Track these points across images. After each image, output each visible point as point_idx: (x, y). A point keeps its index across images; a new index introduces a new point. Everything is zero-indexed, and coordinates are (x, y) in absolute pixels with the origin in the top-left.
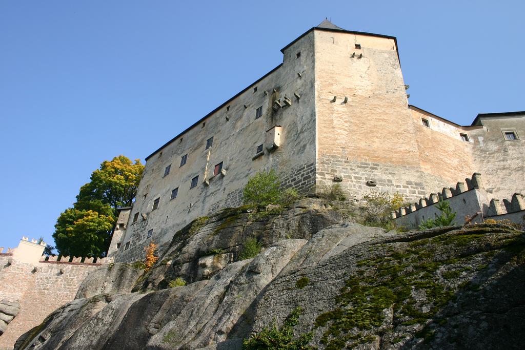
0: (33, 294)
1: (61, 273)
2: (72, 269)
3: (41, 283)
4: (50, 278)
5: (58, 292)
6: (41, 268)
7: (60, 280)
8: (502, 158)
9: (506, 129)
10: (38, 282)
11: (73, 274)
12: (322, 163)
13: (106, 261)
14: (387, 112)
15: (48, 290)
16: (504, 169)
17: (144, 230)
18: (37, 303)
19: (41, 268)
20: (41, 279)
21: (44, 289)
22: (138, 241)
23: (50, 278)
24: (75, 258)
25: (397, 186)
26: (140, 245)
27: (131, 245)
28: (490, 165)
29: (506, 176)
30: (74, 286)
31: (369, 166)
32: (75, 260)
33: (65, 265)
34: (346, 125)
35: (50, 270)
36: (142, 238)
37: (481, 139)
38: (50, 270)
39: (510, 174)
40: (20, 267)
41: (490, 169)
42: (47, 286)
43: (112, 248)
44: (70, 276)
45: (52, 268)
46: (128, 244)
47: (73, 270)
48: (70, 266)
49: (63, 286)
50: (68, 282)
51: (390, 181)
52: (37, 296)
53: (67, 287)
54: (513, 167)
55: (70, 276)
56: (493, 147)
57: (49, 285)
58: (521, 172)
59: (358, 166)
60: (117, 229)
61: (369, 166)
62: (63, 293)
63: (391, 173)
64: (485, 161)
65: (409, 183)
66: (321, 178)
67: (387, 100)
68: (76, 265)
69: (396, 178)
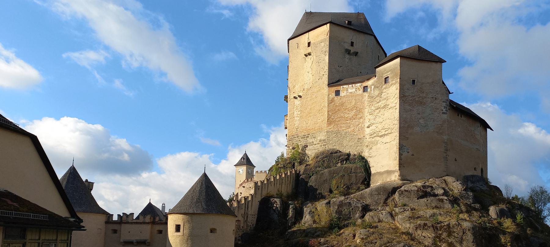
8: (378, 101)
9: (385, 75)
12: (289, 141)
14: (317, 96)
16: (377, 109)
25: (315, 144)
28: (373, 108)
29: (377, 114)
31: (306, 136)
34: (299, 113)
37: (373, 87)
39: (380, 111)
41: (372, 111)
51: (313, 142)
54: (383, 105)
56: (377, 92)
58: (384, 109)
59: (302, 138)
61: (306, 136)
63: (314, 138)
64: (371, 105)
65: (320, 141)
66: (288, 149)
67: (318, 87)
69: (315, 139)
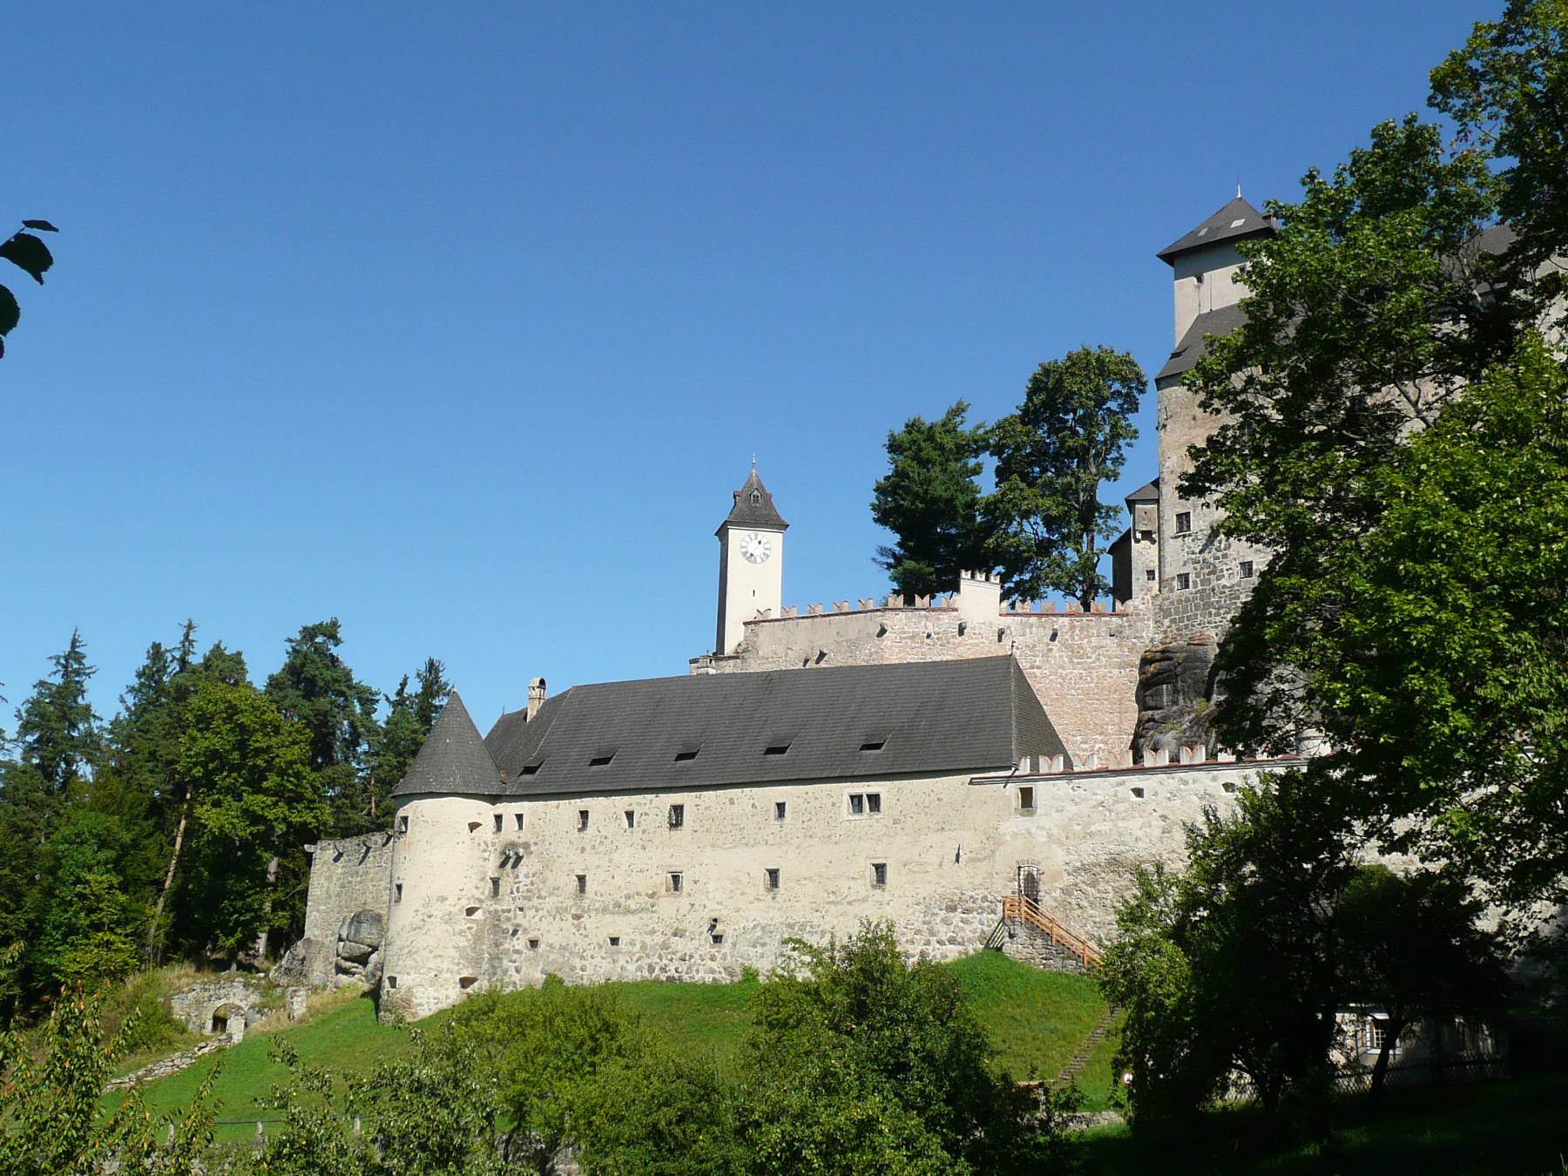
1: (1054, 637)
2: (1072, 628)
4: (1034, 646)
5: (1060, 671)
6: (1009, 627)
13: (1136, 608)
15: (1039, 668)
17: (1225, 556)
19: (1009, 627)
21: (1032, 667)
22: (1213, 577)
23: (1034, 646)
26: (1224, 587)
27: (1195, 583)
30: (1090, 658)
35: (1028, 630)
36: (1225, 573)
38: (1028, 630)
40: (977, 632)
42: (1035, 661)
43: (1138, 579)
44: (1073, 638)
45: (1031, 627)
46: (1184, 579)
49: (1066, 660)
50: (1073, 652)
53: (1075, 660)
55: (1073, 638)
60: (1137, 541)
62: (1071, 673)
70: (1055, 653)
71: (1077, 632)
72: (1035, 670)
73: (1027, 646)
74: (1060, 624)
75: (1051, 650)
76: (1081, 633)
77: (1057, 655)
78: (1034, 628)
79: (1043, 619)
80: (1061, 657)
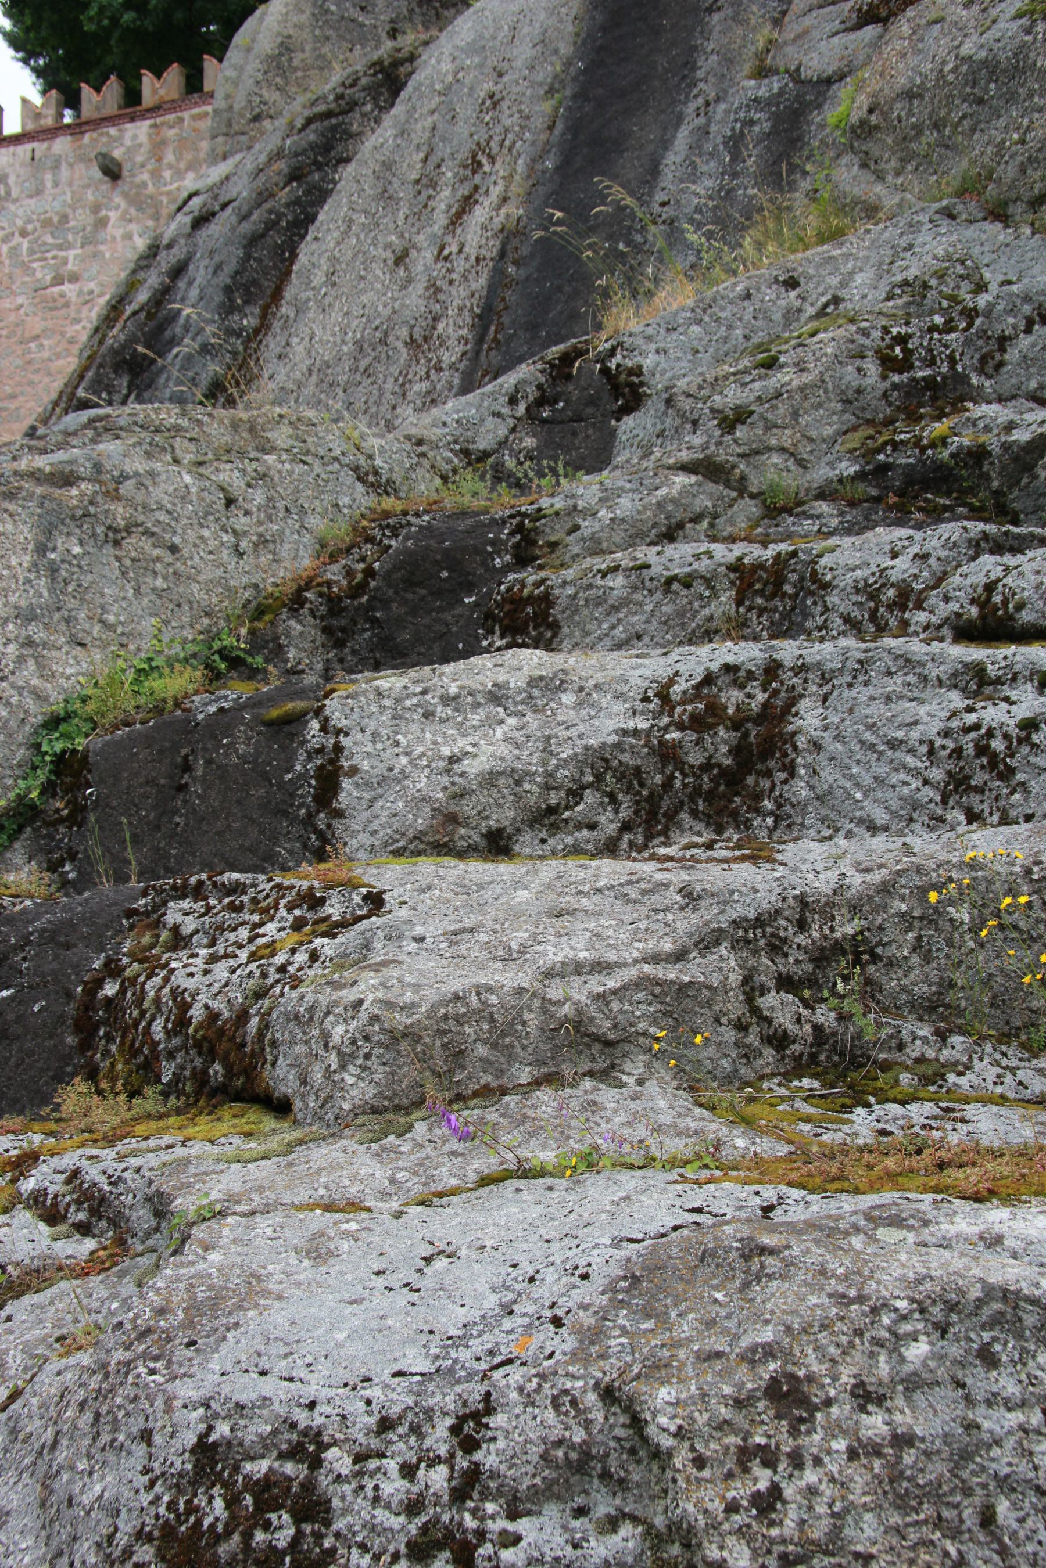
0: (12, 318)
2: (158, 147)
3: (31, 252)
4: (64, 218)
7: (113, 215)
10: (14, 251)
11: (170, 166)
15: (74, 278)
18: (46, 354)
20: (24, 233)
21: (58, 281)
23: (64, 218)
24: (148, 79)
32: (150, 87)
33: (113, 131)
35: (48, 177)
38: (48, 177)
42: (65, 262)
44: (156, 175)
45: (56, 167)
47: (164, 142)
48: (139, 131)
52: (36, 324)
55: (156, 175)
57: (71, 254)
68: (171, 117)
70: (114, 229)
71: (170, 157)
72: (67, 287)
73: (47, 223)
74: (128, 143)
75: (102, 223)
76: (178, 160)
77: (119, 233)
78: (64, 167)
79: (87, 136)
80: (129, 237)
